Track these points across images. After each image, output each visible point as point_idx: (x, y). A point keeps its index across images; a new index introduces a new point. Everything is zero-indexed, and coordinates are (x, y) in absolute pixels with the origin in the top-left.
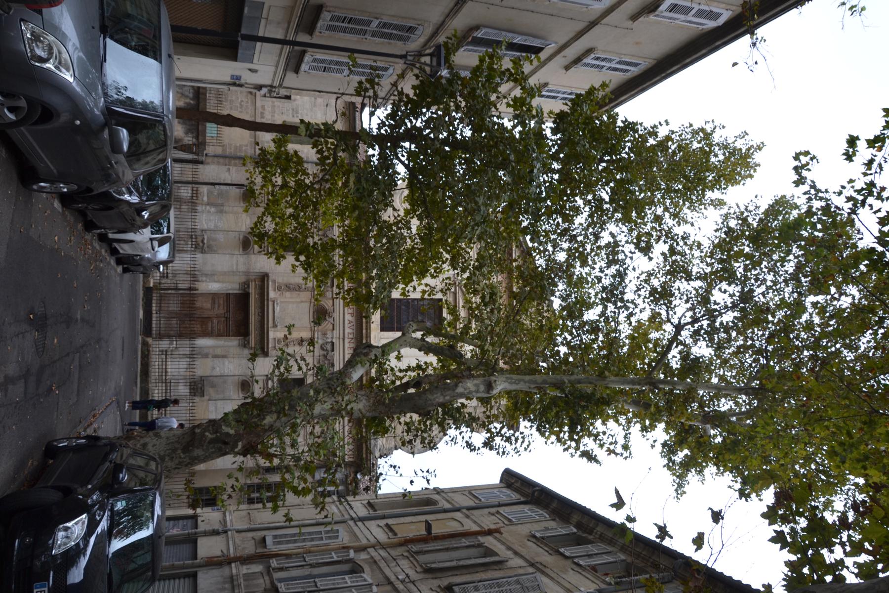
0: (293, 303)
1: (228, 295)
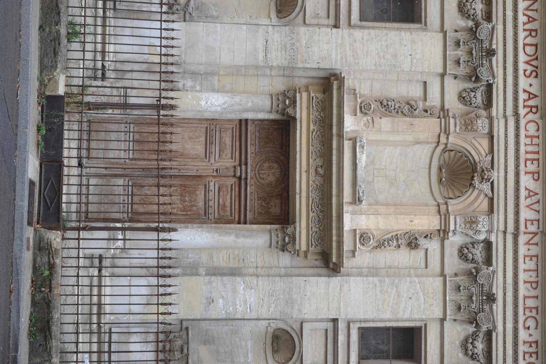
0: (396, 144)
1: (243, 123)
